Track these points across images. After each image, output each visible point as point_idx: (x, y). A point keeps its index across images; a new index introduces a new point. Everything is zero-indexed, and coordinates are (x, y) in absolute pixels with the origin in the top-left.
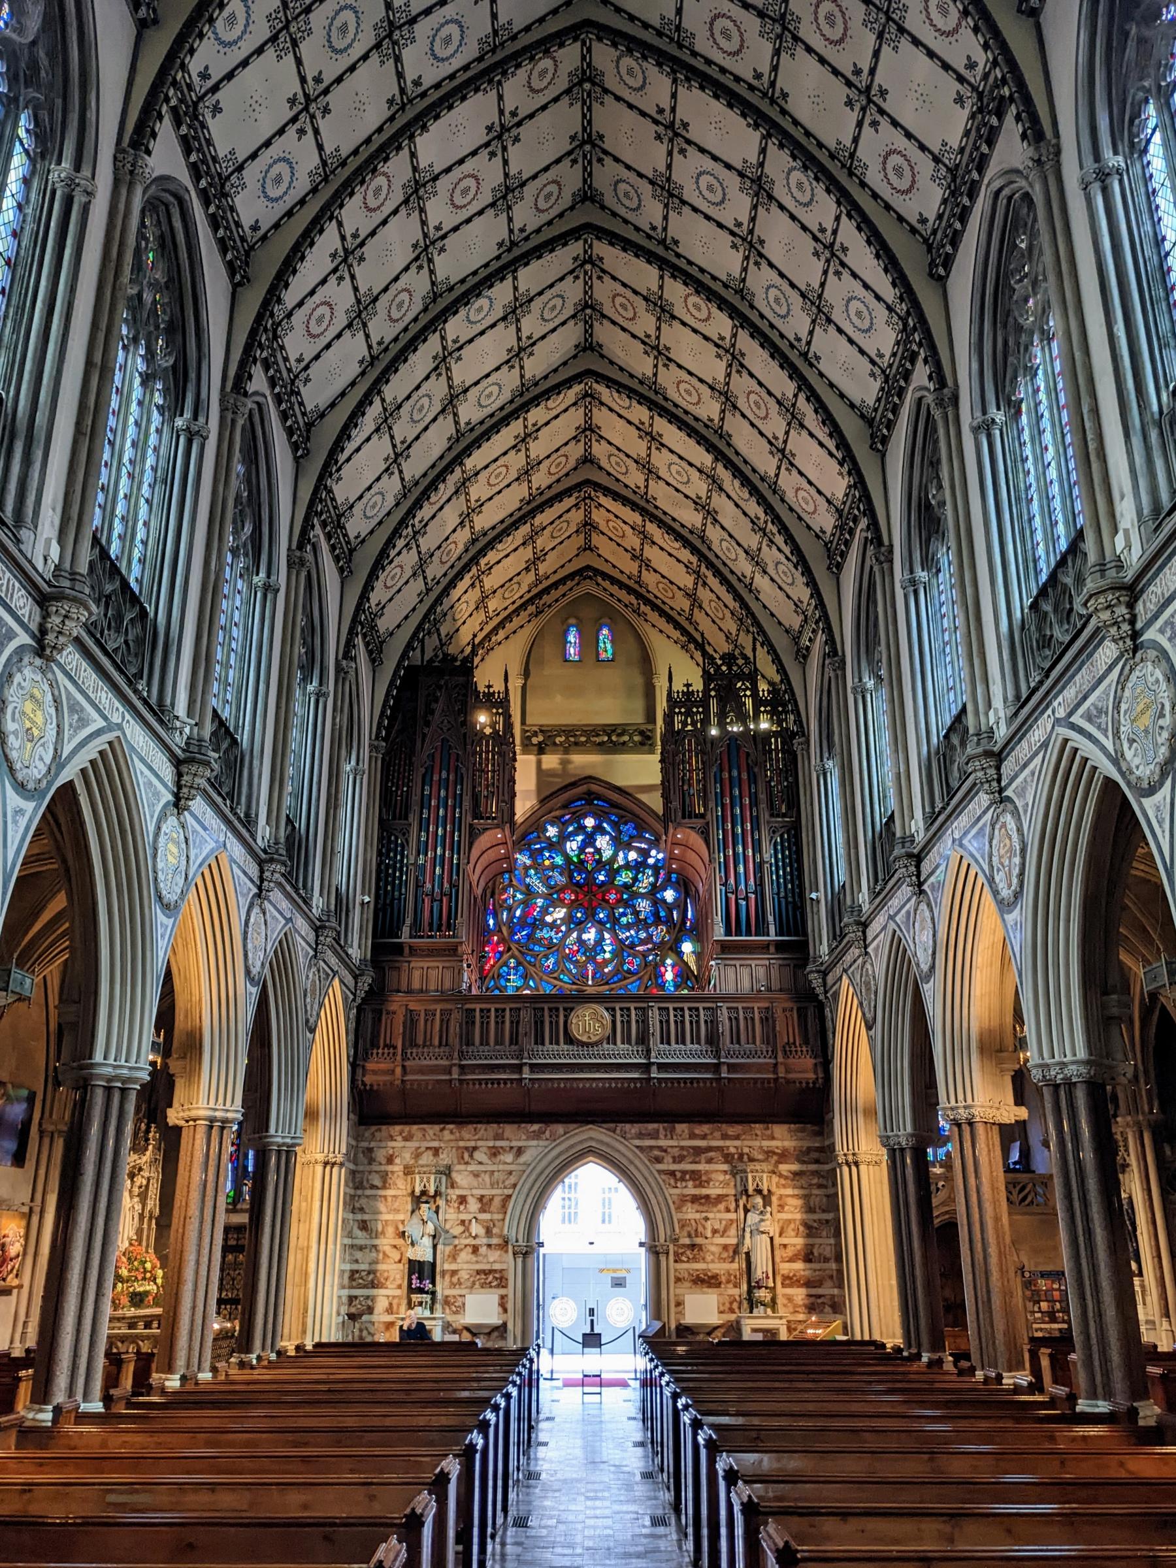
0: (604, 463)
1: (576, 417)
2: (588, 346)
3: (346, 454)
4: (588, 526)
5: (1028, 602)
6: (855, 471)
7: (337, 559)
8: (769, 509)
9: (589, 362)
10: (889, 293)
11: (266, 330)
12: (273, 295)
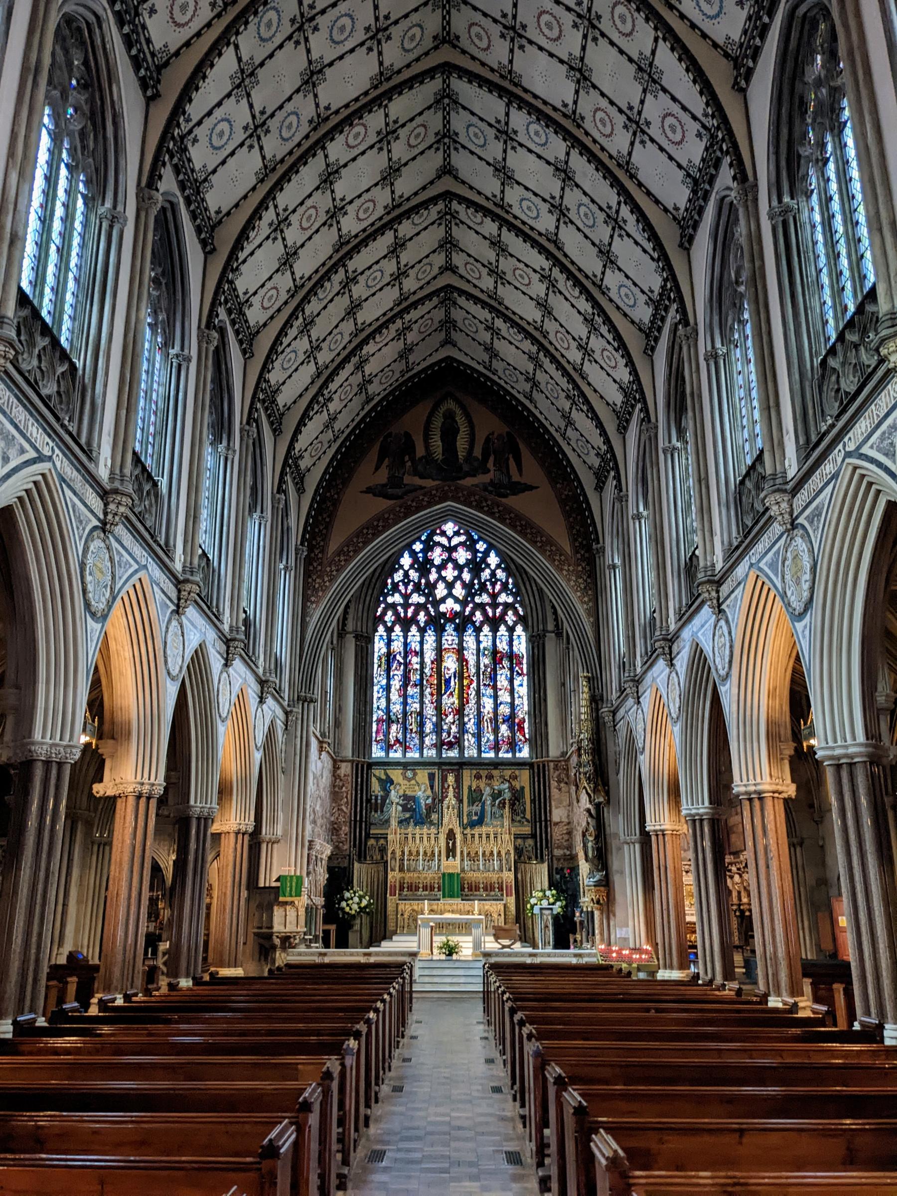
0: (462, 271)
1: (437, 234)
2: (447, 170)
3: (246, 252)
4: (448, 324)
5: (817, 362)
6: (668, 267)
7: (241, 342)
8: (596, 304)
9: (447, 184)
10: (698, 104)
11: (173, 138)
12: (178, 109)
